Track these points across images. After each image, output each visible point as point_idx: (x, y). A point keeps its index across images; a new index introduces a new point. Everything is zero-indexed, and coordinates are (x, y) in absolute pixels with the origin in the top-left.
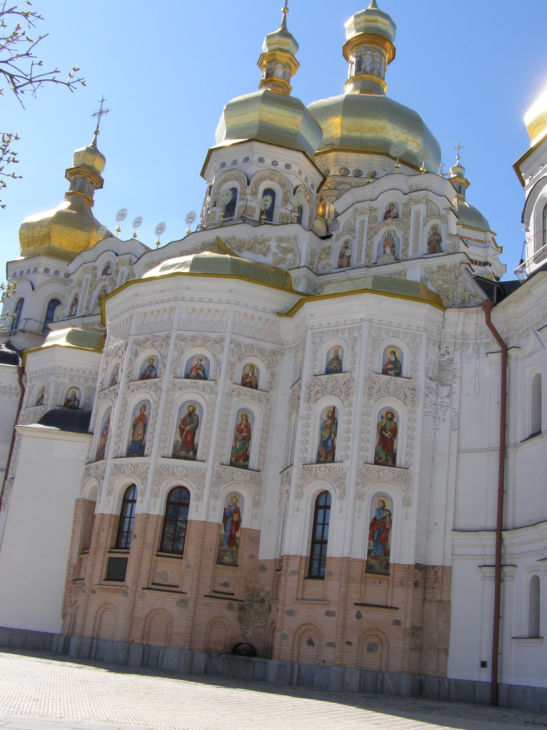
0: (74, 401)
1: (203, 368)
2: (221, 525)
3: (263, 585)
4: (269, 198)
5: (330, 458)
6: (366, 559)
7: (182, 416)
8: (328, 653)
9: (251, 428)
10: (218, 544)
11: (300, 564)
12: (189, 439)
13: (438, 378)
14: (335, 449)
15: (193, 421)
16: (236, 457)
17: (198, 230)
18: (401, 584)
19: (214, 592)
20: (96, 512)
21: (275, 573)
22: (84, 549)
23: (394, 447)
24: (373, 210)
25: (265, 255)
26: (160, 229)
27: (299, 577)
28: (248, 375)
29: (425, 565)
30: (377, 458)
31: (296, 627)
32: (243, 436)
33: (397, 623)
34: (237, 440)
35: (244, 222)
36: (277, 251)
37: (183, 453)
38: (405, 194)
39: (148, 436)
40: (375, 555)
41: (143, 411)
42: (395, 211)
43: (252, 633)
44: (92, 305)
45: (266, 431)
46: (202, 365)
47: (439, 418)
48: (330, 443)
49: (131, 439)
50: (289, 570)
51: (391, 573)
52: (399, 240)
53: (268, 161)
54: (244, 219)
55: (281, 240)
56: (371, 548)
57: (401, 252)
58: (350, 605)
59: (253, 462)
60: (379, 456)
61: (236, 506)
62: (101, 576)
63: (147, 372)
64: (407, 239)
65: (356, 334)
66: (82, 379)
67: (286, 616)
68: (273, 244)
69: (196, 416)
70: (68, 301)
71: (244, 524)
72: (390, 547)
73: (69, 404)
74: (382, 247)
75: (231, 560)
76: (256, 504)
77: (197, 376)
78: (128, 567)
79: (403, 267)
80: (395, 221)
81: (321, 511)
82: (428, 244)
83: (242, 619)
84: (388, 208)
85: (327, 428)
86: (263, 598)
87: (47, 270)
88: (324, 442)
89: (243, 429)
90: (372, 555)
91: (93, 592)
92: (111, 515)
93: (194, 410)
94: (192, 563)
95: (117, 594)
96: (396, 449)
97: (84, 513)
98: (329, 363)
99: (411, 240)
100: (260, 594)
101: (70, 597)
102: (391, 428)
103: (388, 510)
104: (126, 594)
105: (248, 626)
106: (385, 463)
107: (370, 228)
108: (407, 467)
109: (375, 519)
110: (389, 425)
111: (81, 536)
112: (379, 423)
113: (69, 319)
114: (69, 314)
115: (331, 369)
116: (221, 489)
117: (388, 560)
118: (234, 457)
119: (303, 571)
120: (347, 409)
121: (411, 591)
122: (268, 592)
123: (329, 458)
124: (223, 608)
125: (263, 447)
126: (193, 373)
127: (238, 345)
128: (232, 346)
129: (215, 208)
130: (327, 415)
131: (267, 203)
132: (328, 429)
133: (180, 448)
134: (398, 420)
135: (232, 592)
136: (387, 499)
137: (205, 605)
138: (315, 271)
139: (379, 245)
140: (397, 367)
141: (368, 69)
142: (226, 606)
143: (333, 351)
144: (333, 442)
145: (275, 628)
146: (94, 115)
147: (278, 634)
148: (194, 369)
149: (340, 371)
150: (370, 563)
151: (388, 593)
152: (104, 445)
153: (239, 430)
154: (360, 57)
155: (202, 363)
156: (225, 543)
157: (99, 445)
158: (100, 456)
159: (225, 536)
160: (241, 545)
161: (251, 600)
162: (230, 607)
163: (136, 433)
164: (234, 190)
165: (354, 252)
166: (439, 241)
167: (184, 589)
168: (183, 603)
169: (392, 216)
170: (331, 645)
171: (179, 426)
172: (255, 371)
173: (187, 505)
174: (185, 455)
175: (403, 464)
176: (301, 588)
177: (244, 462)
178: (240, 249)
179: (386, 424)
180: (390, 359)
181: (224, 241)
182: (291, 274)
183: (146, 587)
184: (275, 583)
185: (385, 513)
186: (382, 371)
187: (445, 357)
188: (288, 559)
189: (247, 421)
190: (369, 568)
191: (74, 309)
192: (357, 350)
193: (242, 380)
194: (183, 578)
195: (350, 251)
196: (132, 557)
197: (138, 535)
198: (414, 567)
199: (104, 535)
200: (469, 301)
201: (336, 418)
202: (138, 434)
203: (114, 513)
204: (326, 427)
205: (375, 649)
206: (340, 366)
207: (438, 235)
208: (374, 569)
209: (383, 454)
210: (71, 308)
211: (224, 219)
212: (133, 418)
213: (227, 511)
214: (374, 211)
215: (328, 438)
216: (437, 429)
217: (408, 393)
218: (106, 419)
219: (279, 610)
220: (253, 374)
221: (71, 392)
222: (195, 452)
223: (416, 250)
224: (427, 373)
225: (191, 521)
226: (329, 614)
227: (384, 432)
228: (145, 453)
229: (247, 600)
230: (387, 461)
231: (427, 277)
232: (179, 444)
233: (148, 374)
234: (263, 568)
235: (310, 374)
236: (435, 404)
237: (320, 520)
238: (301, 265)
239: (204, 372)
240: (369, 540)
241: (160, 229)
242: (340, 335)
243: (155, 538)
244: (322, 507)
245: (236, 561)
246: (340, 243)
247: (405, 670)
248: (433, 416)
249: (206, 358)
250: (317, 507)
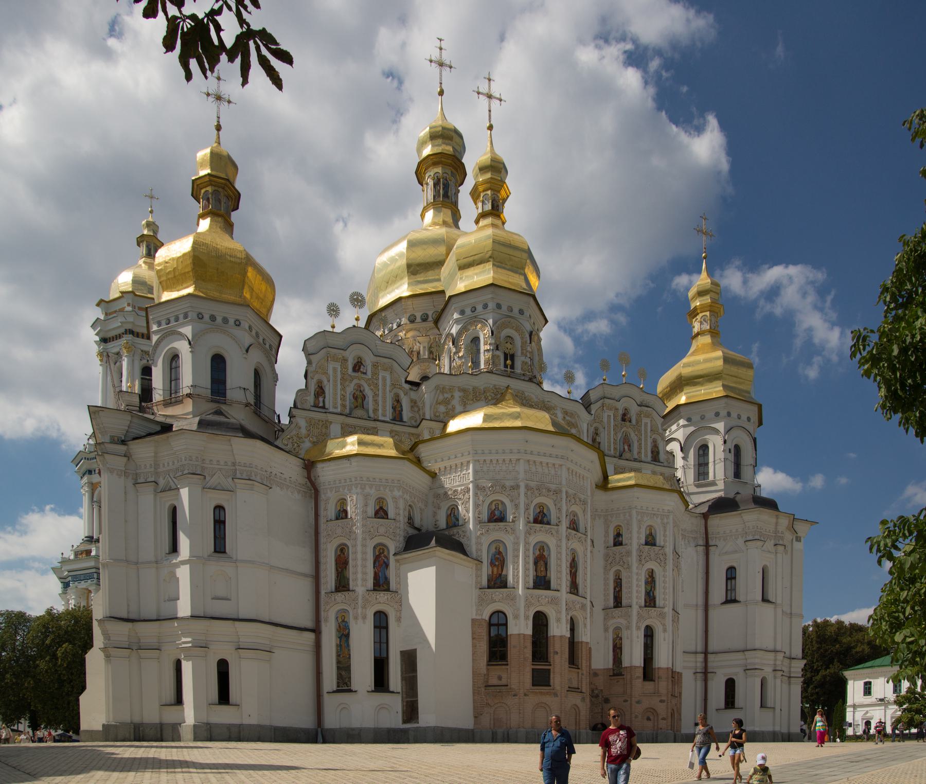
44: (348, 403)
48: (652, 594)
55: (566, 413)
91: (525, 695)
95: (547, 696)
98: (647, 537)
104: (556, 695)
113: (325, 412)
114: (315, 403)
122: (602, 690)
143: (648, 529)
149: (654, 545)
167: (584, 690)
168: (583, 699)
170: (663, 719)
191: (321, 399)
192: (667, 533)
225: (582, 642)
226: (662, 701)
242: (655, 518)
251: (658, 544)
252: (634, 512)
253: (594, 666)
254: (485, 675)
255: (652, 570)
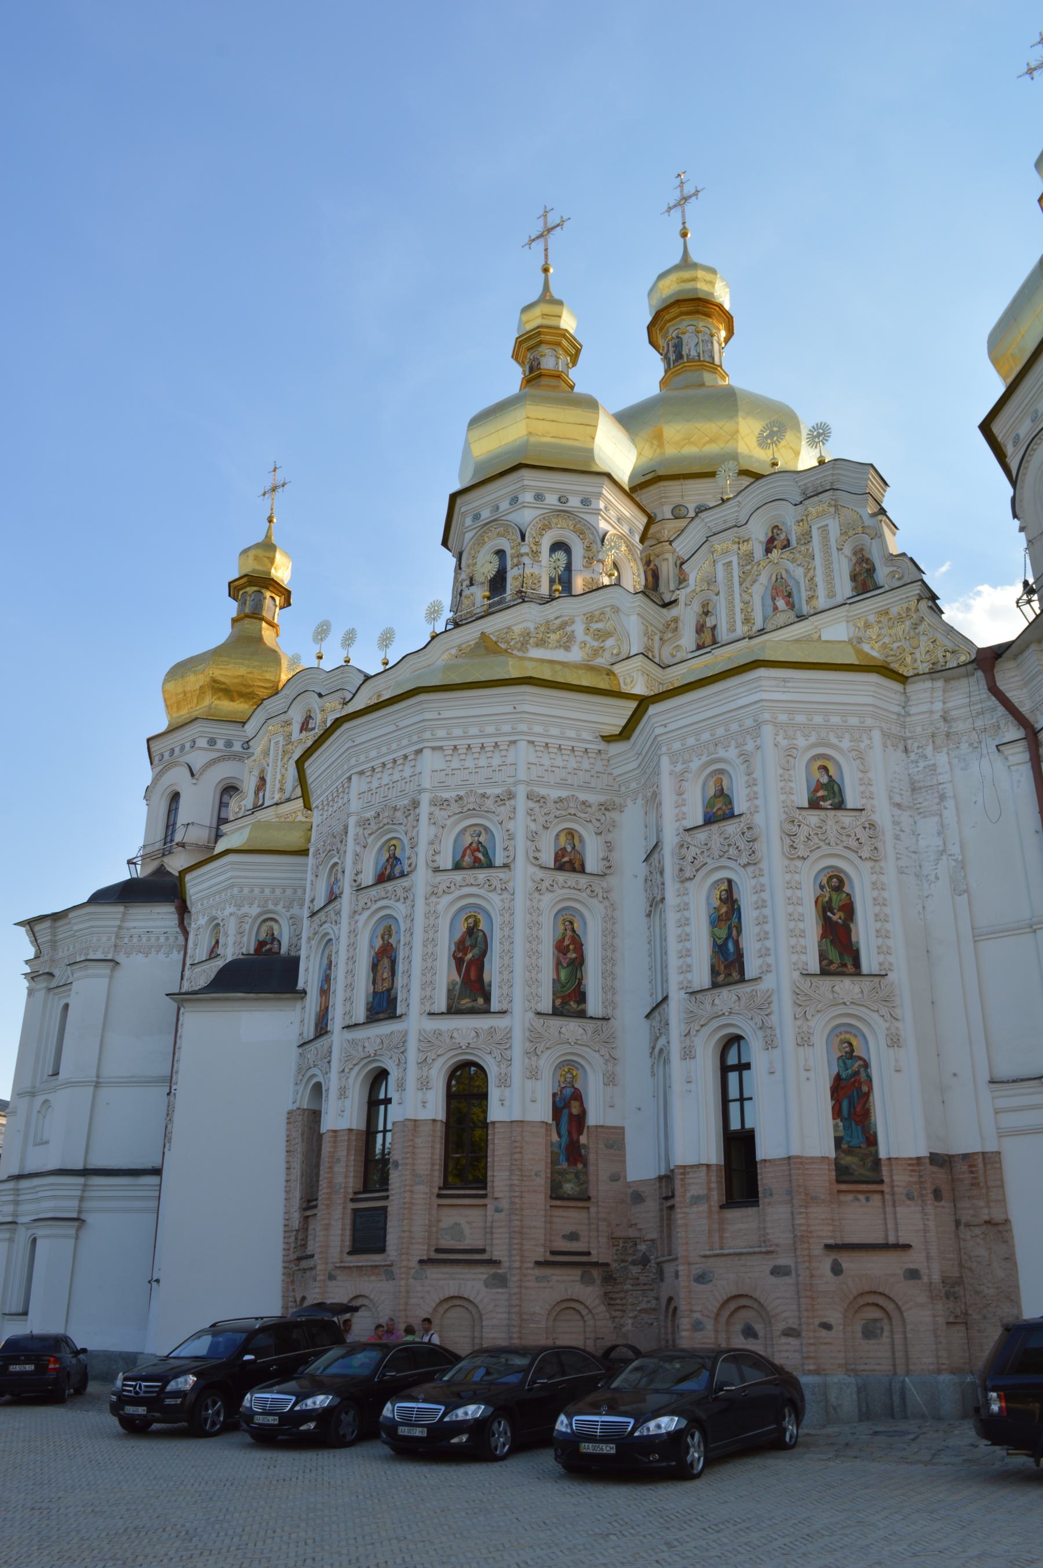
0: (272, 943)
1: (484, 847)
2: (551, 1125)
3: (640, 1229)
4: (561, 555)
5: (735, 975)
6: (832, 1154)
7: (458, 936)
8: (787, 1351)
9: (583, 942)
10: (549, 1161)
11: (709, 1182)
12: (473, 976)
13: (911, 805)
14: (742, 956)
15: (476, 942)
16: (563, 998)
17: (449, 627)
18: (910, 1197)
19: (553, 1253)
20: (323, 1130)
21: (661, 1204)
22: (309, 1201)
23: (854, 939)
24: (743, 542)
25: (567, 648)
26: (386, 639)
27: (710, 1207)
28: (564, 849)
29: (947, 1155)
30: (825, 962)
31: (718, 1305)
32: (570, 959)
33: (913, 1274)
34: (560, 967)
35: (524, 601)
36: (588, 639)
37: (466, 1003)
38: (796, 505)
39: (400, 980)
40: (849, 1147)
41: (386, 937)
42: (783, 536)
43: (633, 1324)
45: (609, 946)
46: (480, 843)
47: (927, 876)
48: (731, 946)
49: (371, 991)
50: (688, 1195)
51: (886, 1179)
52: (798, 583)
53: (551, 499)
54: (522, 597)
55: (590, 618)
56: (841, 1134)
57: (804, 602)
58: (818, 1250)
59: (594, 1005)
60: (828, 959)
61: (573, 1086)
62: (342, 1246)
63: (386, 869)
64: (812, 579)
65: (750, 746)
66: (282, 903)
67: (695, 1284)
68: (579, 628)
69: (481, 934)
70: (249, 785)
71: (592, 1120)
72: (876, 1128)
73: (264, 949)
74: (769, 602)
75: (577, 1189)
76: (610, 1080)
77: (475, 862)
78: (389, 1224)
79: (813, 626)
80: (786, 554)
81: (733, 1077)
82: (851, 580)
83: (611, 1299)
84: (770, 535)
85: (722, 920)
86: (644, 1254)
87: (212, 742)
88: (720, 947)
89: (568, 946)
90: (844, 1146)
91: (331, 1277)
92: (350, 1130)
93: (476, 922)
94: (504, 1204)
95: (373, 1278)
96: (858, 942)
97: (303, 1134)
98: (709, 805)
99: (819, 579)
100: (639, 1247)
101: (294, 1290)
102: (841, 904)
103: (860, 1058)
105: (623, 1311)
106: (840, 969)
107: (743, 573)
108: (883, 973)
109: (838, 1079)
110: (837, 900)
111: (302, 1176)
112: (817, 898)
113: (253, 813)
114: (254, 804)
115: (714, 813)
116: (542, 1062)
117: (877, 1152)
118: (558, 998)
119: (715, 1193)
120: (754, 882)
121: (930, 1209)
122: (653, 1241)
123: (734, 974)
124: (573, 1281)
125: (609, 974)
126: (467, 858)
127: (541, 800)
128: (531, 804)
129: (473, 589)
130: (718, 896)
131: (559, 563)
132: (723, 923)
133: (459, 994)
134: (852, 887)
135: (586, 1250)
136: (855, 1036)
137: (538, 1279)
138: (657, 660)
139: (763, 599)
140: (834, 793)
141: (693, 353)
142: (578, 1278)
144: (737, 944)
145: (675, 1309)
146: (264, 494)
147: (684, 1323)
148: (468, 852)
149: (732, 816)
150: (843, 1162)
151: (885, 1219)
152: (327, 1008)
153: (560, 948)
154: (678, 337)
155: (481, 839)
156: (562, 1158)
157: (318, 1010)
158: (322, 1028)
159: (560, 1145)
160: (592, 1157)
161: (623, 1261)
162: (587, 1280)
163: (378, 977)
164: (500, 553)
165: (721, 619)
166: (871, 571)
167: (497, 1255)
169: (779, 546)
170: (789, 1332)
171: (453, 955)
172: (576, 842)
173: (484, 1096)
174: (469, 1005)
175: (875, 970)
176: (716, 1226)
177: (578, 1005)
178: (524, 646)
179: (830, 899)
180: (818, 781)
181: (494, 639)
182: (616, 672)
183: (425, 1258)
184: (665, 1222)
185: (856, 1065)
186: (809, 804)
187: (919, 764)
188: (683, 1174)
189: (573, 931)
190: (843, 1174)
191: (261, 795)
193: (556, 860)
194: (492, 1233)
195: (713, 618)
196: (394, 1207)
197: (400, 1162)
198: (927, 1161)
199: (339, 1169)
200: (946, 662)
201: (736, 901)
202: (383, 980)
203: (354, 1127)
204: (720, 918)
205: (879, 1331)
206: (729, 807)
207: (867, 561)
208: (852, 1174)
209: (833, 955)
210: (256, 794)
211: (489, 602)
212: (370, 952)
213: (558, 1099)
214: (746, 543)
215: (726, 939)
216: (927, 897)
217: (863, 836)
218: (325, 962)
219: (680, 1273)
220: (574, 847)
221: (264, 928)
222: (487, 999)
223: (831, 594)
224: (890, 798)
225: (493, 1123)
226: (777, 1271)
227: (829, 914)
228: (398, 1013)
229: (616, 1261)
230: (844, 965)
231: (860, 635)
232: (458, 987)
233: (387, 872)
234: (638, 1198)
235: (677, 829)
236: (915, 852)
237: (733, 1092)
238: (631, 654)
239: (486, 854)
240: (834, 1118)
241: (386, 639)
243: (433, 1165)
244: (733, 1068)
245: (587, 1189)
246: (696, 607)
247: (944, 1367)
248: (915, 874)
249: (486, 829)
250: (725, 1069)
251: (736, 814)
252: (665, 761)
253: (629, 1179)
254: (297, 1231)
255: (730, 882)
